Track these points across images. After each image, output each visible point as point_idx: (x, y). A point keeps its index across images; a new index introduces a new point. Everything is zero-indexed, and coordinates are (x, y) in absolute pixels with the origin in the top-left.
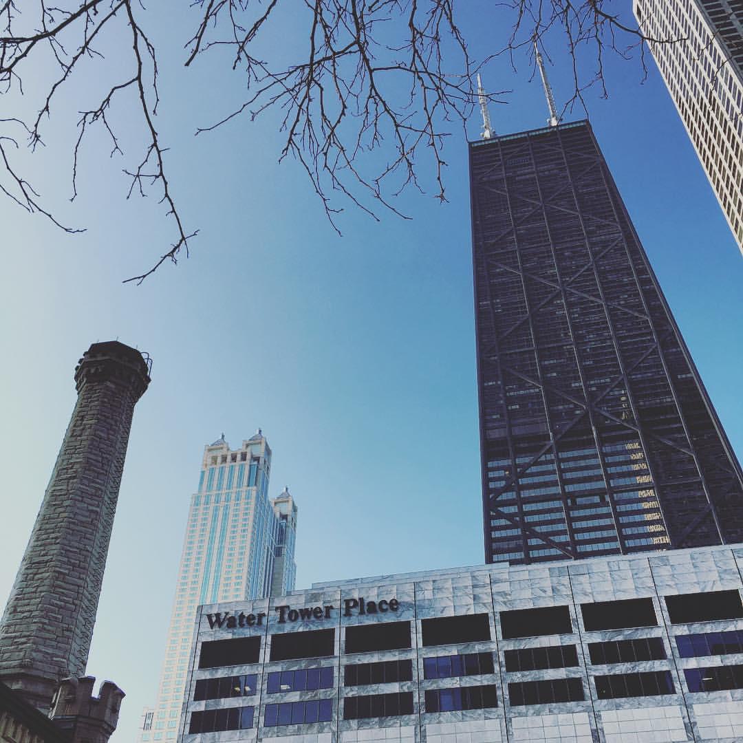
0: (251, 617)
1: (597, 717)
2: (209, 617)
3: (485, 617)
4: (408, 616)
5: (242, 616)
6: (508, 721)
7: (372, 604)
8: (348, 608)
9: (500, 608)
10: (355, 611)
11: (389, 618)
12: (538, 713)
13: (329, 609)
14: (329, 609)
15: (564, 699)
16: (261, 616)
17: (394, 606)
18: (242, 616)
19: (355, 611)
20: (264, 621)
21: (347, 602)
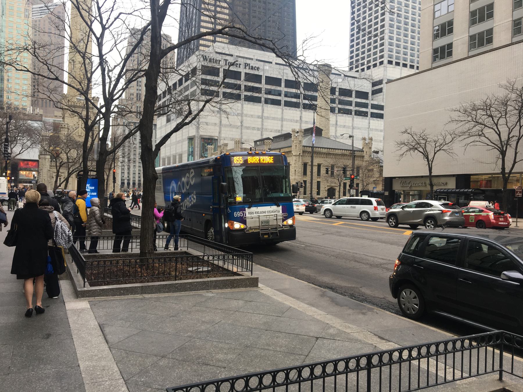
0: (216, 60)
1: (301, 113)
2: (203, 56)
3: (281, 79)
4: (261, 73)
5: (213, 59)
6: (283, 110)
7: (252, 67)
8: (245, 66)
9: (285, 78)
10: (247, 67)
11: (256, 73)
12: (289, 109)
13: (240, 64)
14: (240, 64)
15: (295, 107)
16: (220, 61)
17: (258, 69)
18: (213, 59)
19: (247, 67)
20: (220, 62)
21: (245, 64)
